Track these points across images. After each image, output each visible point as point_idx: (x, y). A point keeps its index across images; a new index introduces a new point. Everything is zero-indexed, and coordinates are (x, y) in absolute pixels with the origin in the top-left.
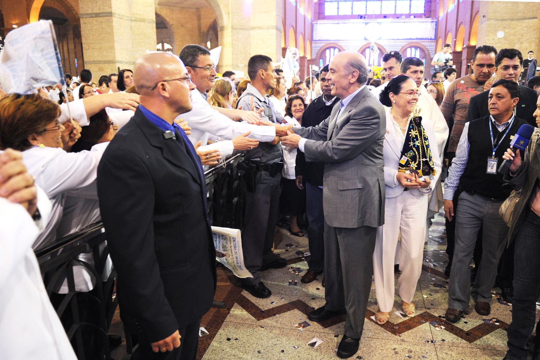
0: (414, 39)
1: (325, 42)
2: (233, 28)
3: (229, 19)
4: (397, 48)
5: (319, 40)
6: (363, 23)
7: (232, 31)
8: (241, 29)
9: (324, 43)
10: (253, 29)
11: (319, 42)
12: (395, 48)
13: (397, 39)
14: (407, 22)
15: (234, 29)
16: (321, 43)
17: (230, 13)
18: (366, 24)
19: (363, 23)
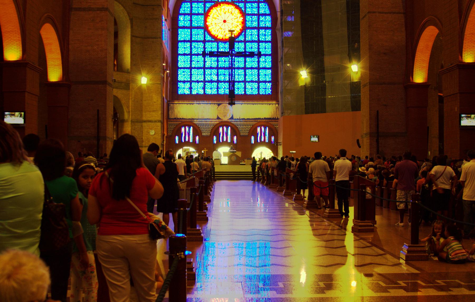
0: (262, 119)
1: (180, 120)
2: (132, 122)
3: (129, 116)
4: (248, 126)
5: (175, 119)
6: (216, 104)
7: (131, 123)
8: (137, 122)
9: (180, 121)
10: (145, 121)
11: (174, 120)
12: (246, 126)
13: (247, 119)
14: (256, 104)
15: (133, 122)
16: (176, 121)
17: (130, 112)
18: (219, 105)
19: (216, 104)
